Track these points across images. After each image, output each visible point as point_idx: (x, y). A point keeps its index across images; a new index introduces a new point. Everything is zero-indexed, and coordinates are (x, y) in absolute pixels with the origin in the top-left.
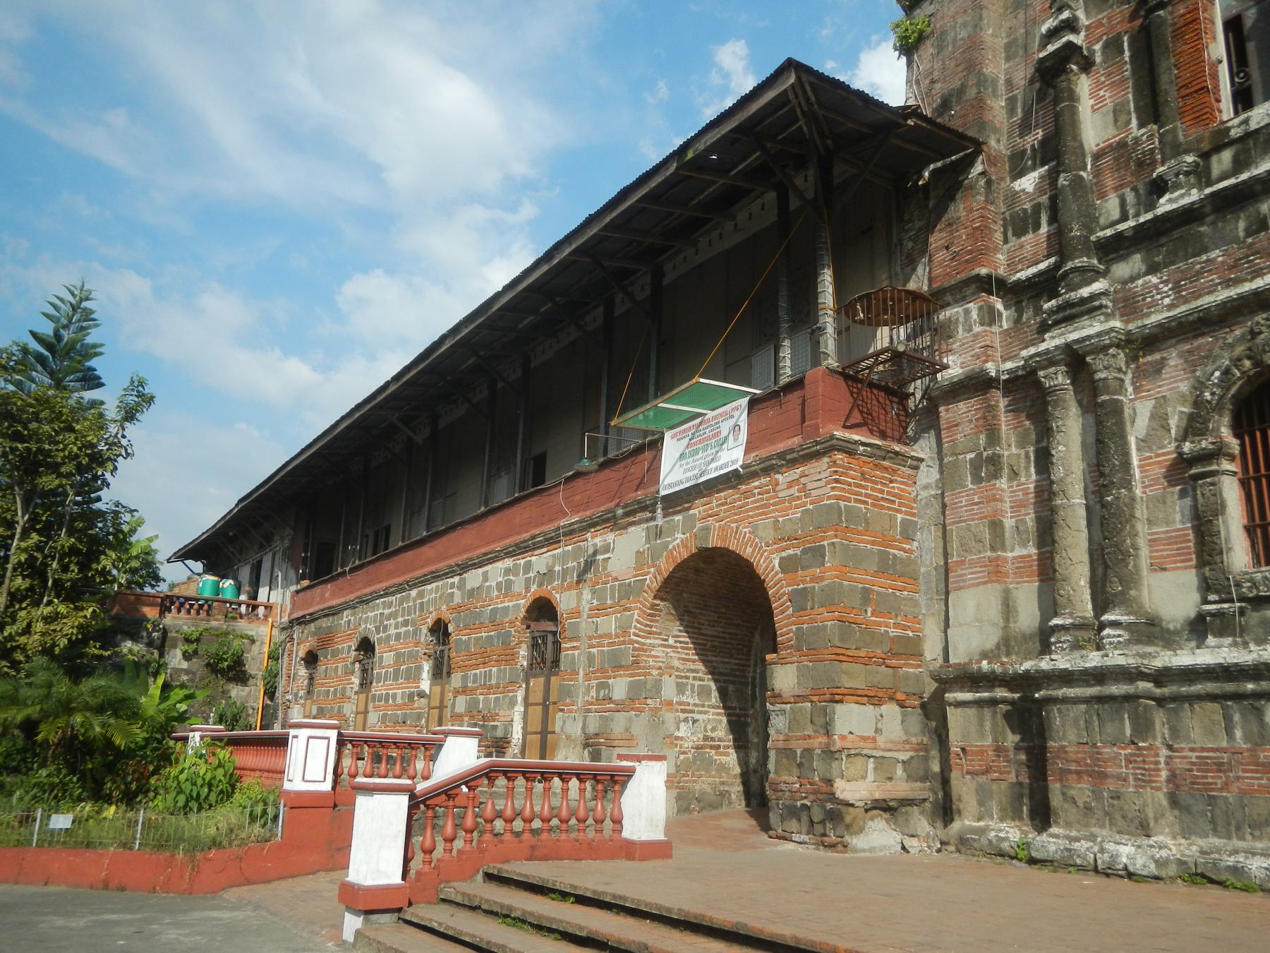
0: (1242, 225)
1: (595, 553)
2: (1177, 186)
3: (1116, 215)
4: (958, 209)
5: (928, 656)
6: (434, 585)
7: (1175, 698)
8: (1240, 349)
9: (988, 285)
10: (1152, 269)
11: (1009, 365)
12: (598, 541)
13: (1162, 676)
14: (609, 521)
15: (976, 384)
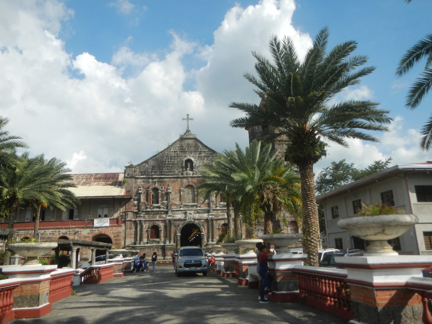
0: (153, 213)
1: (78, 231)
2: (149, 208)
3: (143, 208)
4: (129, 203)
5: (122, 244)
6: (24, 231)
7: (146, 248)
8: (152, 223)
9: (132, 211)
10: (146, 214)
11: (134, 220)
12: (79, 230)
13: (145, 246)
14: (83, 228)
15: (131, 221)
